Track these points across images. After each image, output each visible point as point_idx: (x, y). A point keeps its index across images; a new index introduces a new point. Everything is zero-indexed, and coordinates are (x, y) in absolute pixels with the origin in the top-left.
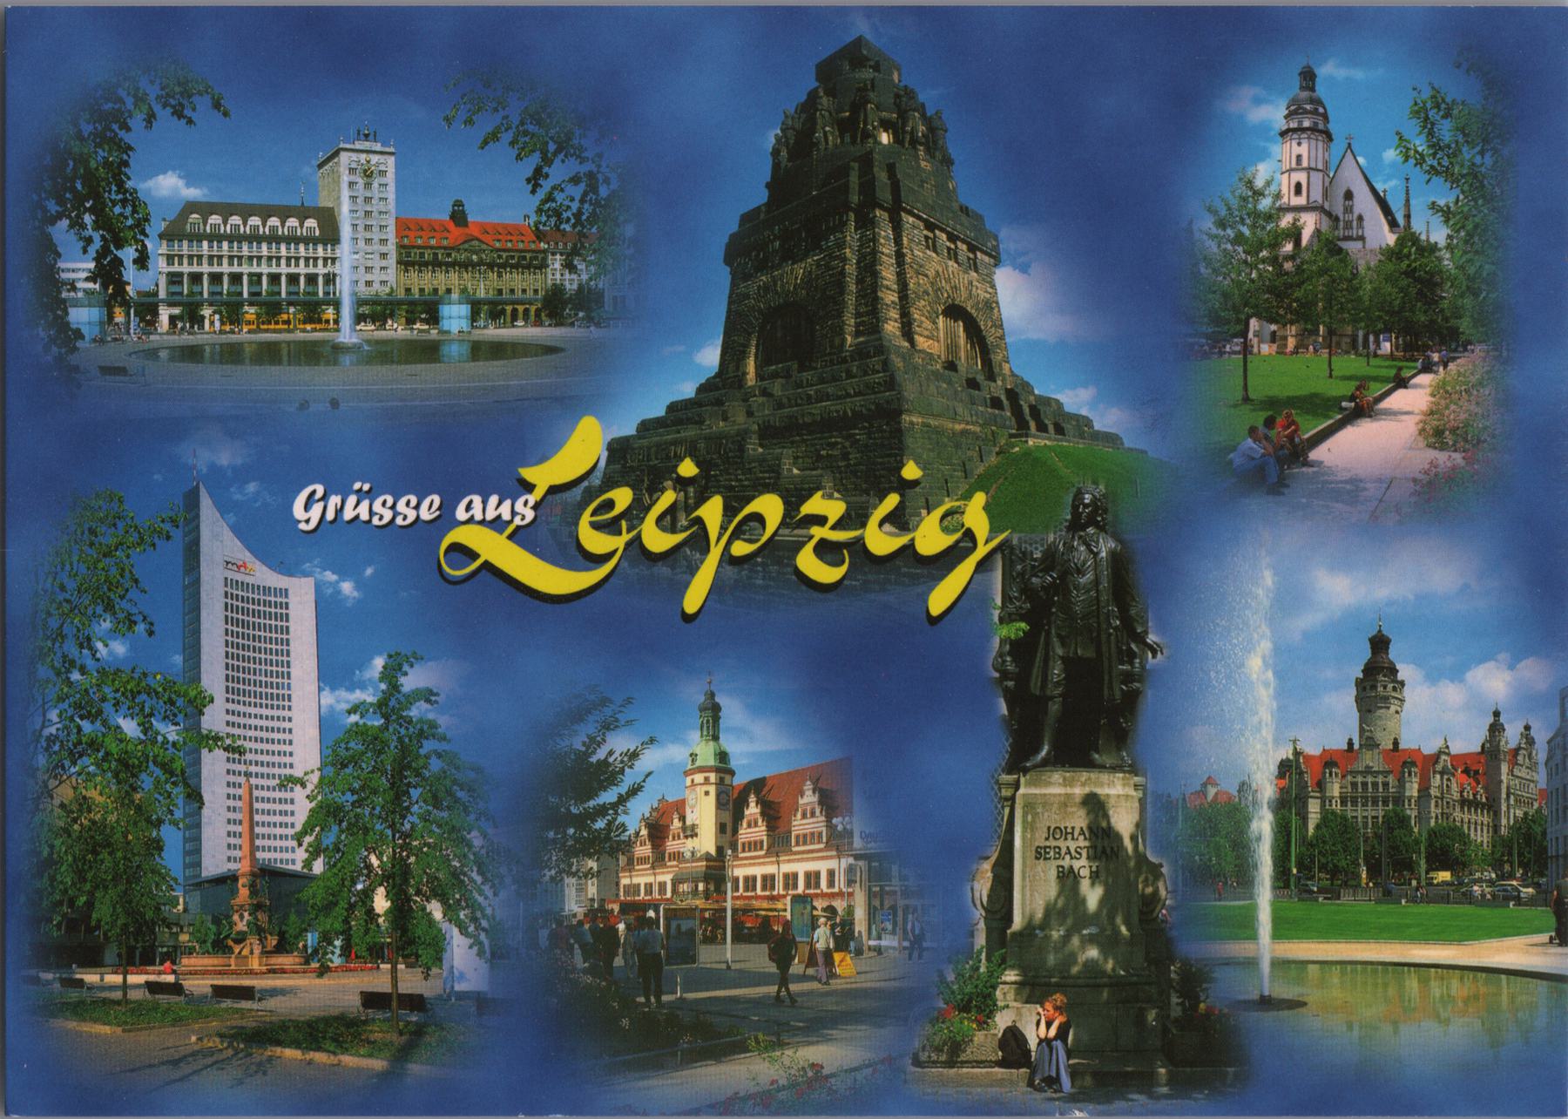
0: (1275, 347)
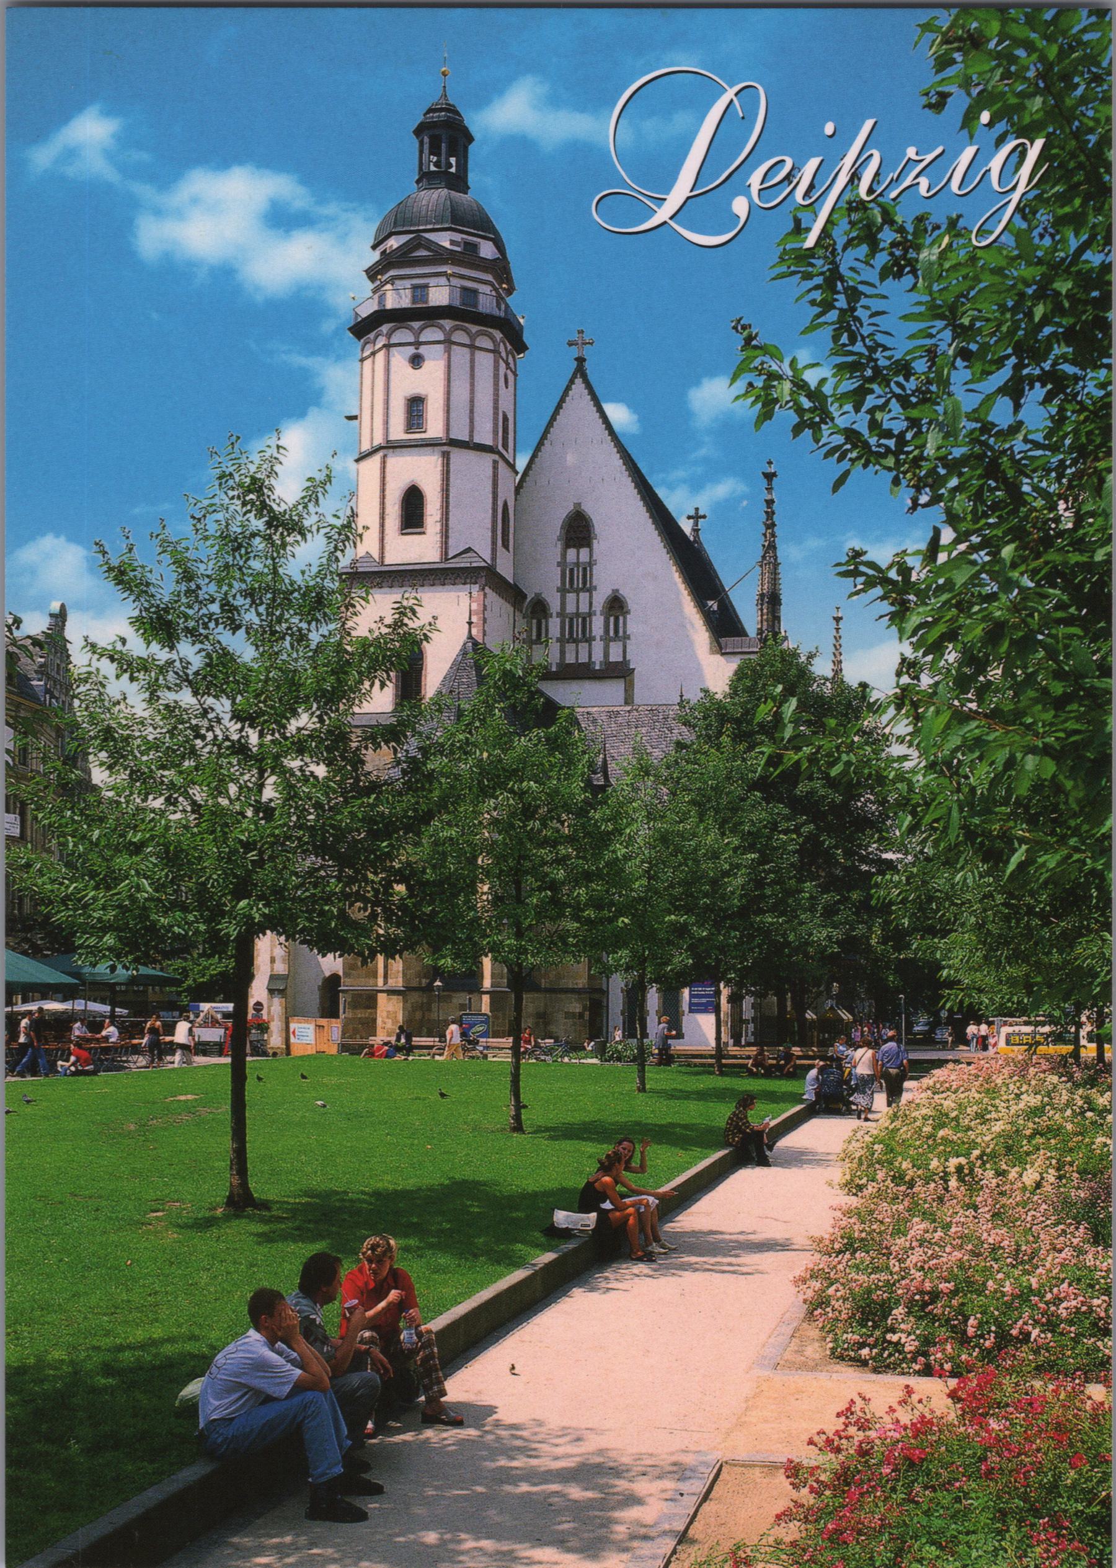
0: (335, 1028)
